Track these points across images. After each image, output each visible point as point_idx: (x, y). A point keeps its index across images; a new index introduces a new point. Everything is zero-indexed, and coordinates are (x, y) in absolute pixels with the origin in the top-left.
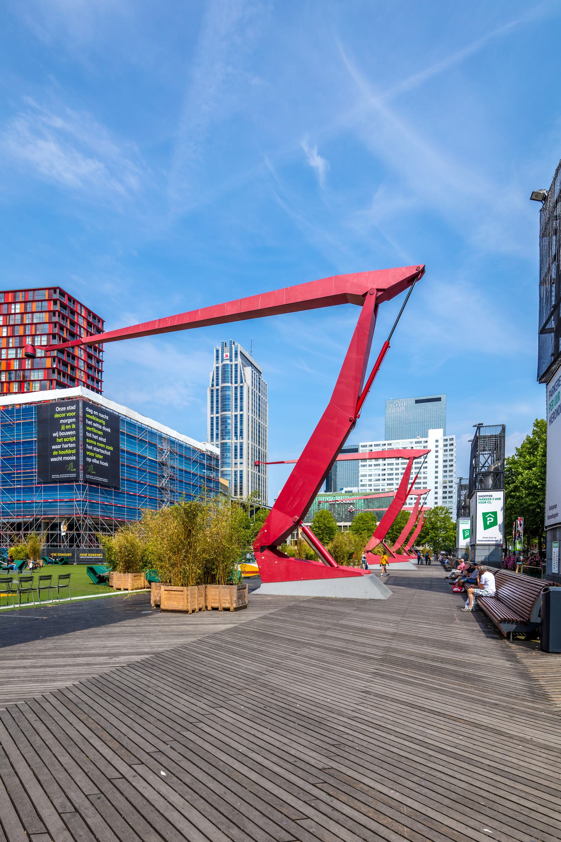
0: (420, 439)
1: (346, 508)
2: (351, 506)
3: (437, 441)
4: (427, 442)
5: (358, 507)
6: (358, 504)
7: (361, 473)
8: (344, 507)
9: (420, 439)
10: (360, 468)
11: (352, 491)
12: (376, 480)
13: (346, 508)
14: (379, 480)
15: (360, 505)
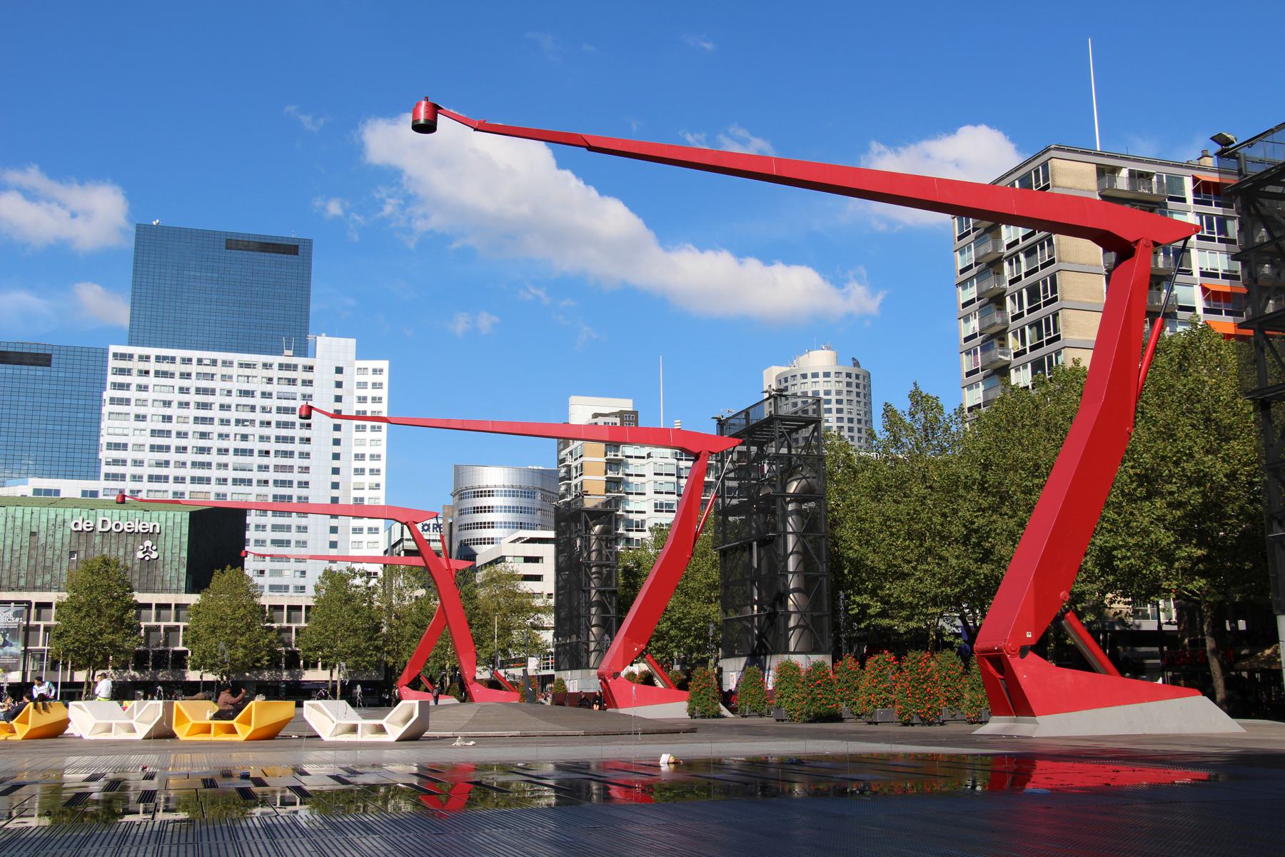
0: (294, 360)
1: (129, 548)
2: (148, 543)
3: (339, 370)
4: (311, 368)
5: (169, 545)
6: (169, 539)
7: (104, 440)
8: (122, 544)
9: (294, 360)
10: (105, 424)
11: (57, 492)
12: (159, 464)
13: (129, 548)
14: (167, 463)
15: (177, 542)
